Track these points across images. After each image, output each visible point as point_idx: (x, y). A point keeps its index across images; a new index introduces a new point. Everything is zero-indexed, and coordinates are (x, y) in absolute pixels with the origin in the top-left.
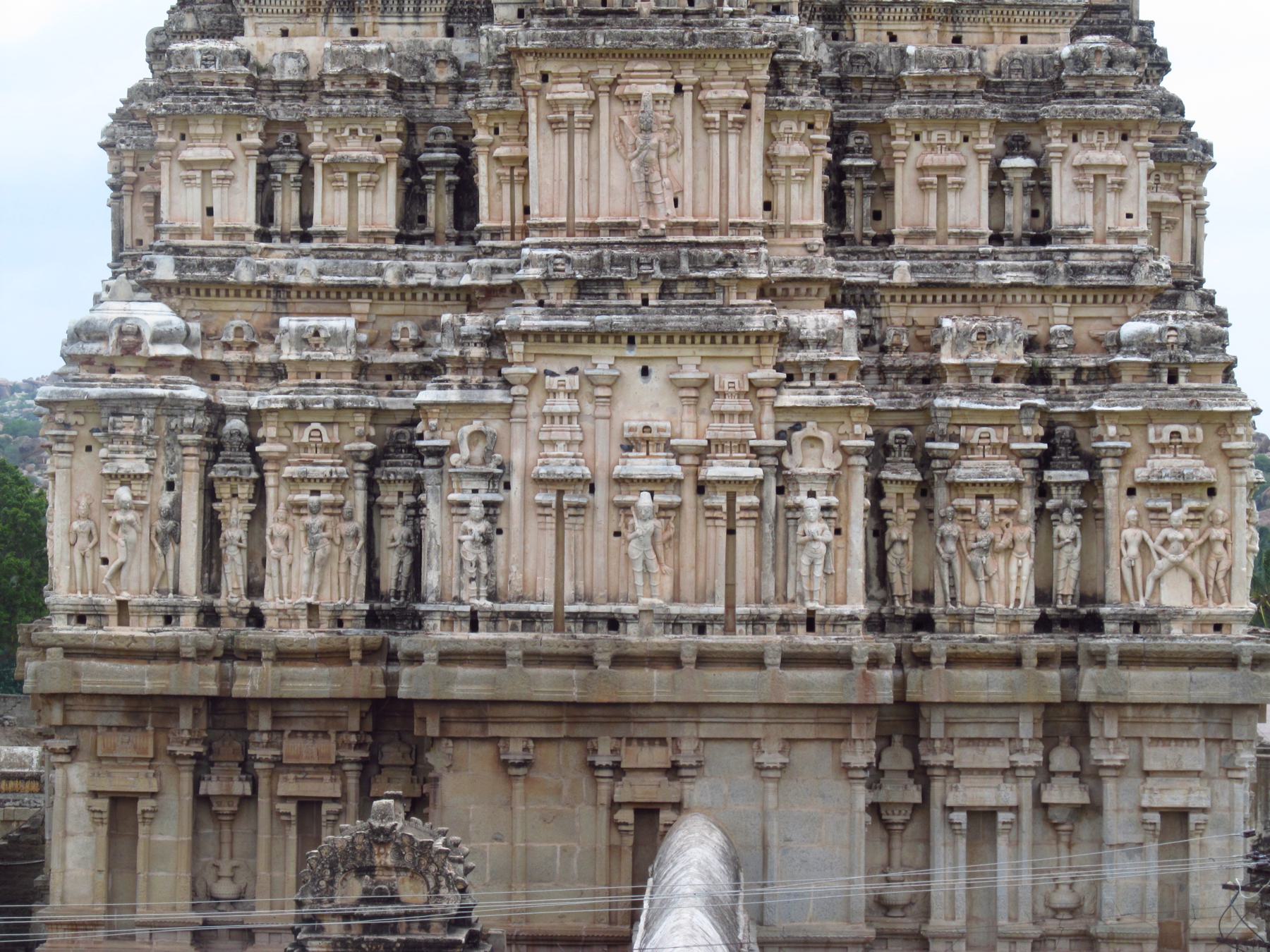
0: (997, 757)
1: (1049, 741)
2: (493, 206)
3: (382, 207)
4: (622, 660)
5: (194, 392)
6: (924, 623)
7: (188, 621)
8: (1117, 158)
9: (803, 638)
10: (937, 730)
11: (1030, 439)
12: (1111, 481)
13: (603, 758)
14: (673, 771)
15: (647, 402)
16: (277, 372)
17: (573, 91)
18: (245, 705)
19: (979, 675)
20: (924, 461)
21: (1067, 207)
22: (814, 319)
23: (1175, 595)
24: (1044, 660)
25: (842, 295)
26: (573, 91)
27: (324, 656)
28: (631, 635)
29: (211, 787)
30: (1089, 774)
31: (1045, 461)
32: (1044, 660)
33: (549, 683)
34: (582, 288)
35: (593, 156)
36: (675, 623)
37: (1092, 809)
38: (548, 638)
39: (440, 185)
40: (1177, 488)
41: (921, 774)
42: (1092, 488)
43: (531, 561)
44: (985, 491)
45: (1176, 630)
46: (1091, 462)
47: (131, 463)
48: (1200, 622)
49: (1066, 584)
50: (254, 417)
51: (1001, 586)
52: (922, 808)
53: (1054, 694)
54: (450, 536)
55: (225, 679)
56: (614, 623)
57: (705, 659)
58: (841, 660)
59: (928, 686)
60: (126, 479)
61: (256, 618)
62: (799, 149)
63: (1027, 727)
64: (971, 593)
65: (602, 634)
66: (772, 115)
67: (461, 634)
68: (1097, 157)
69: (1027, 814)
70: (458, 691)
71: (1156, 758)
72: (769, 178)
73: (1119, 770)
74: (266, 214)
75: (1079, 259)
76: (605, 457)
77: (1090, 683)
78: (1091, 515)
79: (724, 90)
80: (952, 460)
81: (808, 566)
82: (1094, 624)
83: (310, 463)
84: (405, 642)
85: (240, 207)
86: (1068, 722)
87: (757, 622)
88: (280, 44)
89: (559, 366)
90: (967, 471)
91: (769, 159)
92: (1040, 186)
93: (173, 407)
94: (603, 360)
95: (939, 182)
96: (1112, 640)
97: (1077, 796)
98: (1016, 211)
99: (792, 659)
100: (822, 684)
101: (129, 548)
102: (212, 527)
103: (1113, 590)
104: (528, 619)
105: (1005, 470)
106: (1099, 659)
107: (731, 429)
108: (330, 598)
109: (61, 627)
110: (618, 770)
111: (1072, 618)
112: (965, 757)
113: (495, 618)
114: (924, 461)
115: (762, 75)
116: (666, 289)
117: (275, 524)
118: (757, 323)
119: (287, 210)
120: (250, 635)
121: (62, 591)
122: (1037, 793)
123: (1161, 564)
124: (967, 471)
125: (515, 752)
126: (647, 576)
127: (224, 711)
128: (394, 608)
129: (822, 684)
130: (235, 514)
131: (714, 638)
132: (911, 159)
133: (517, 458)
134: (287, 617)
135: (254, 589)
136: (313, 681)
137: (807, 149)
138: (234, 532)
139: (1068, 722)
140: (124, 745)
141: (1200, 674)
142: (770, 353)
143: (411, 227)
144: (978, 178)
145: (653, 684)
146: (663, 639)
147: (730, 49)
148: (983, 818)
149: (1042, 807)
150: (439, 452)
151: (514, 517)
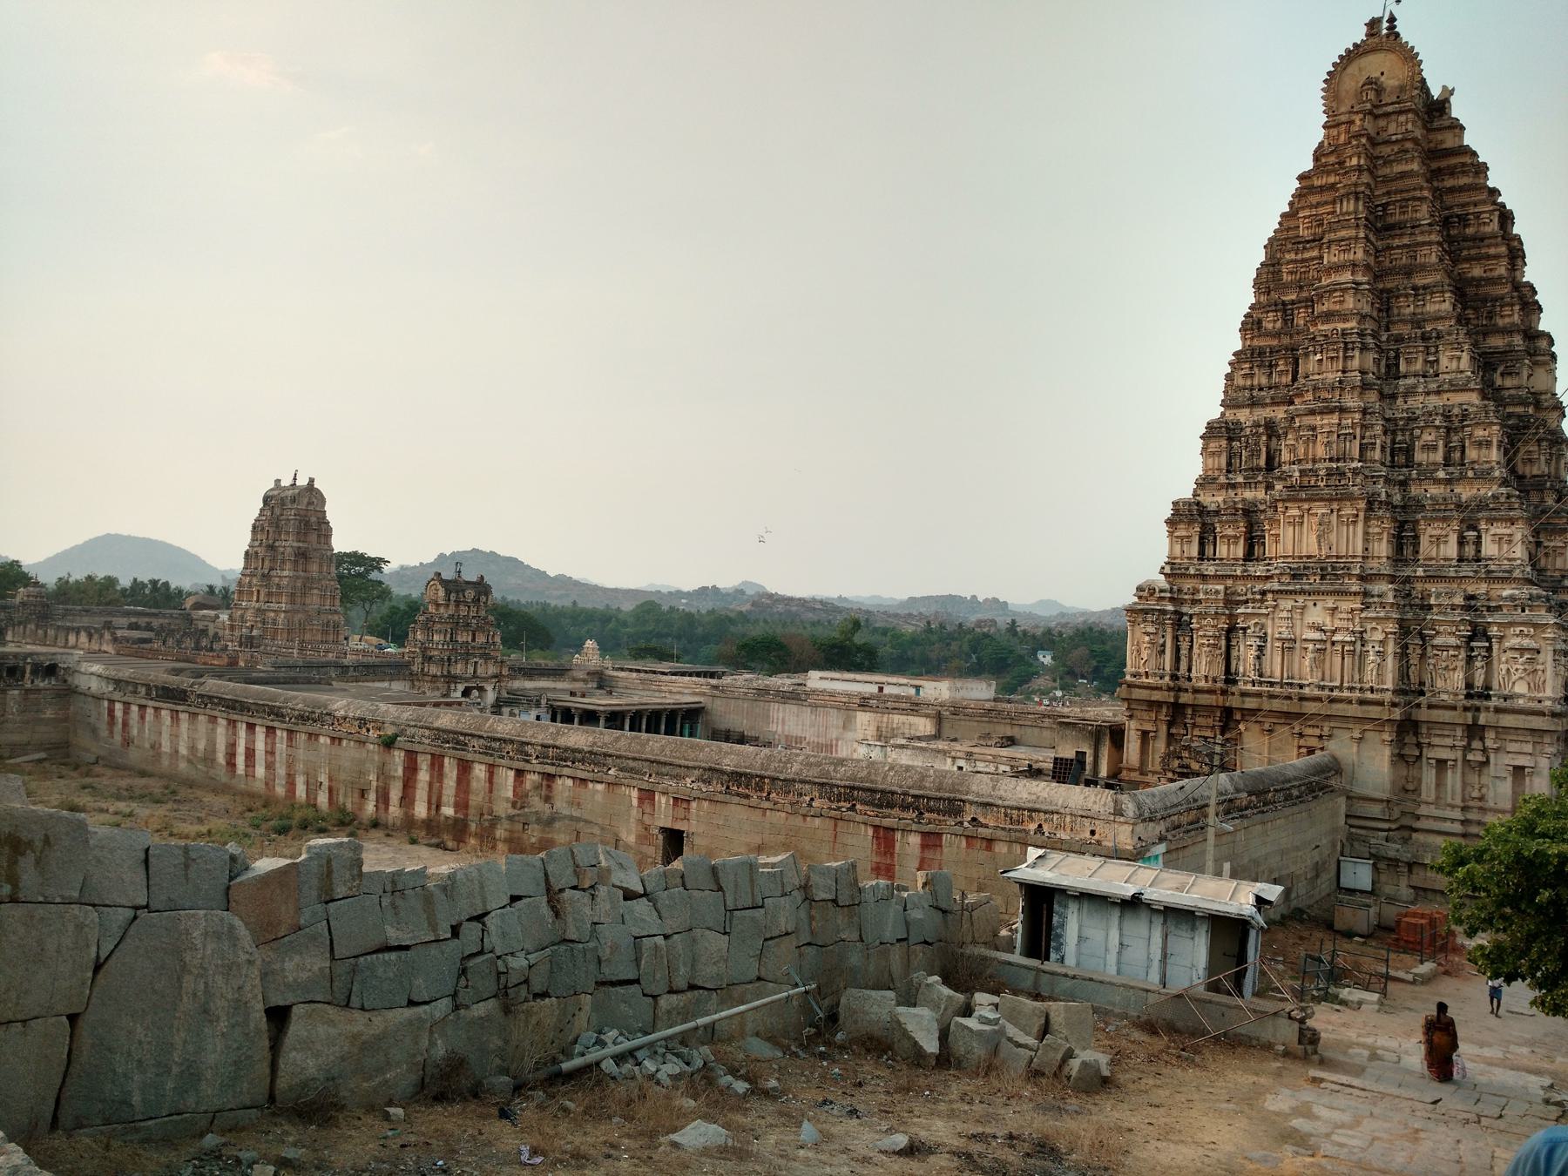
0: (1449, 741)
1: (1470, 738)
3: (1239, 551)
4: (1302, 699)
5: (1170, 608)
6: (1422, 693)
7: (1167, 678)
8: (1508, 531)
9: (1369, 695)
10: (1424, 730)
11: (1465, 631)
12: (1495, 647)
13: (1297, 730)
14: (1321, 737)
15: (1317, 614)
17: (1295, 512)
18: (1184, 706)
19: (1440, 712)
20: (1422, 637)
21: (1489, 548)
23: (1521, 688)
24: (1466, 709)
25: (1392, 579)
26: (1295, 512)
27: (1210, 692)
28: (1306, 691)
29: (1173, 731)
31: (1471, 639)
32: (1466, 709)
33: (1276, 705)
34: (1294, 577)
35: (1301, 533)
36: (1323, 688)
37: (1487, 762)
38: (1277, 689)
40: (1522, 650)
41: (1419, 745)
42: (1489, 649)
43: (1274, 665)
44: (1446, 648)
45: (1521, 701)
46: (1489, 639)
47: (1151, 629)
48: (1531, 699)
49: (1479, 681)
50: (1191, 616)
51: (1450, 682)
52: (1419, 757)
53: (1470, 722)
54: (1246, 654)
55: (1177, 698)
56: (1301, 686)
57: (1333, 701)
58: (1380, 703)
59: (1423, 715)
60: (1148, 634)
61: (1190, 679)
62: (1377, 530)
63: (1459, 732)
64: (1440, 684)
65: (1297, 690)
66: (1367, 519)
67: (1249, 687)
68: (1499, 531)
69: (1459, 763)
70: (1247, 706)
71: (1513, 747)
72: (1366, 540)
73: (1497, 750)
74: (1202, 552)
75: (1493, 568)
77: (1483, 719)
79: (1348, 511)
80: (1433, 637)
81: (1370, 668)
82: (1488, 697)
83: (1206, 632)
84: (1234, 689)
86: (1474, 731)
87: (1351, 689)
88: (1210, 499)
89: (1287, 604)
90: (1438, 641)
91: (1366, 533)
92: (1478, 542)
93: (1163, 612)
94: (1301, 599)
95: (1438, 540)
96: (1494, 702)
97: (1480, 757)
98: (1470, 551)
99: (1362, 702)
100: (1374, 712)
102: (1177, 650)
103: (1495, 685)
104: (1272, 684)
105: (1452, 641)
106: (1487, 709)
107: (1344, 624)
108: (1211, 675)
109: (1128, 678)
110: (1301, 735)
111: (1477, 694)
112: (1436, 741)
113: (1261, 683)
114: (1422, 637)
115: (1362, 505)
116: (1323, 577)
117: (1196, 650)
118: (1354, 588)
119: (1209, 551)
120: (1187, 685)
121: (1129, 669)
122: (1464, 756)
123: (1514, 678)
124: (1438, 641)
125: (1267, 726)
128: (1230, 678)
130: (1184, 646)
131: (1336, 693)
132: (1428, 532)
133: (1269, 631)
134: (1198, 679)
135: (1190, 670)
136: (1204, 699)
137: (1383, 528)
138: (1184, 652)
139: (1474, 731)
140: (1145, 716)
141: (1530, 718)
142: (1359, 599)
144: (1453, 538)
145: (1311, 708)
146: (1317, 692)
147: (1350, 498)
148: (1441, 764)
149: (1466, 761)
150: (1244, 629)
151: (1268, 651)
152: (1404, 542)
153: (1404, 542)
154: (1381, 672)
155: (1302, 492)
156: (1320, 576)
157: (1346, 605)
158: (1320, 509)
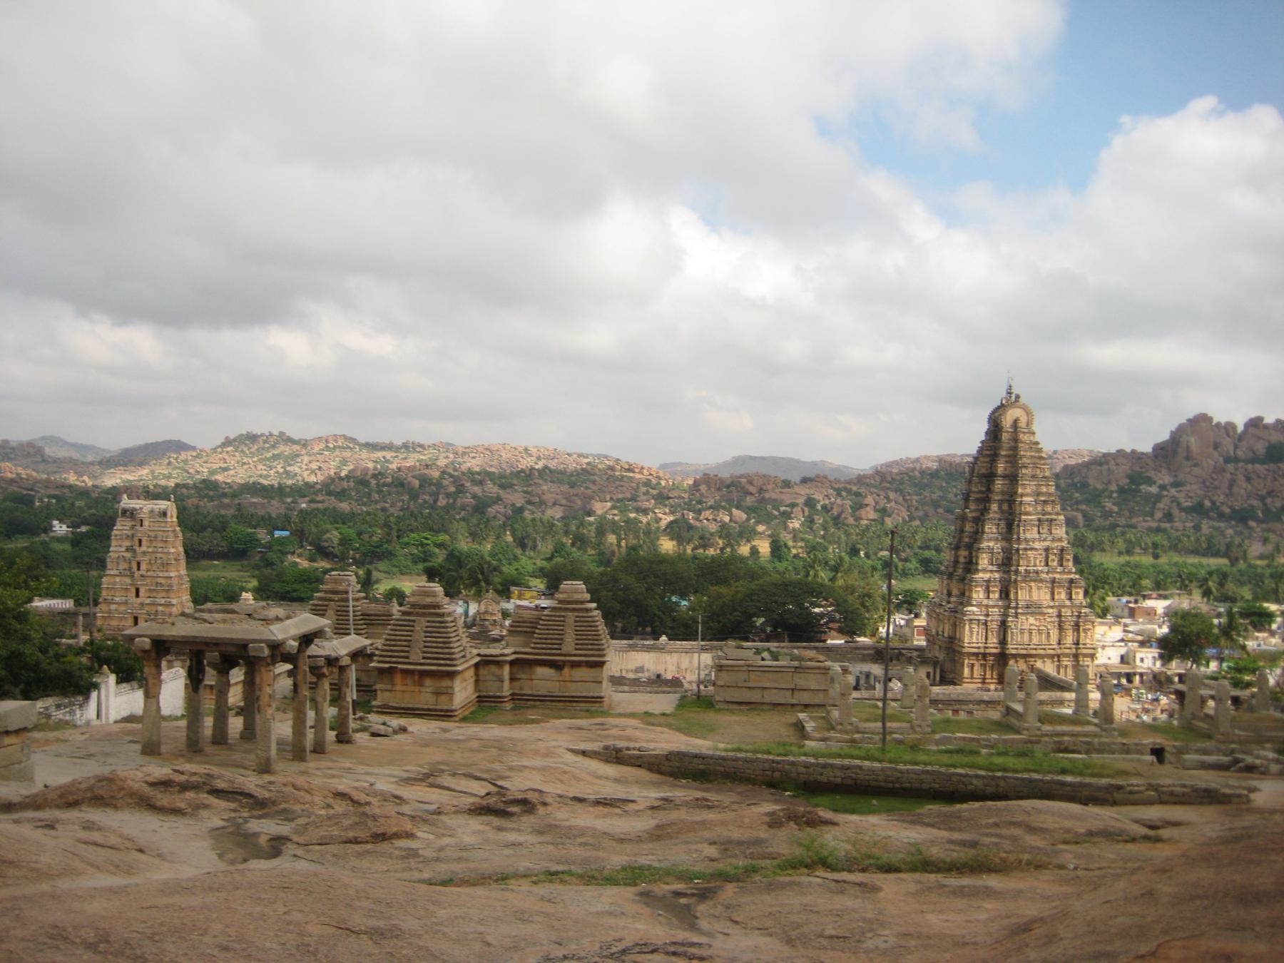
2: (1012, 596)
3: (997, 595)
15: (1032, 620)
22: (1050, 611)
33: (1024, 652)
85: (981, 595)
86: (1076, 656)
92: (1071, 594)
95: (1059, 593)
127: (985, 655)
128: (1003, 642)
129: (1052, 652)
139: (1076, 656)
143: (1001, 598)
145: (1033, 652)
147: (1041, 581)
152: (1053, 593)
153: (1053, 593)
156: (1033, 608)
158: (1032, 584)
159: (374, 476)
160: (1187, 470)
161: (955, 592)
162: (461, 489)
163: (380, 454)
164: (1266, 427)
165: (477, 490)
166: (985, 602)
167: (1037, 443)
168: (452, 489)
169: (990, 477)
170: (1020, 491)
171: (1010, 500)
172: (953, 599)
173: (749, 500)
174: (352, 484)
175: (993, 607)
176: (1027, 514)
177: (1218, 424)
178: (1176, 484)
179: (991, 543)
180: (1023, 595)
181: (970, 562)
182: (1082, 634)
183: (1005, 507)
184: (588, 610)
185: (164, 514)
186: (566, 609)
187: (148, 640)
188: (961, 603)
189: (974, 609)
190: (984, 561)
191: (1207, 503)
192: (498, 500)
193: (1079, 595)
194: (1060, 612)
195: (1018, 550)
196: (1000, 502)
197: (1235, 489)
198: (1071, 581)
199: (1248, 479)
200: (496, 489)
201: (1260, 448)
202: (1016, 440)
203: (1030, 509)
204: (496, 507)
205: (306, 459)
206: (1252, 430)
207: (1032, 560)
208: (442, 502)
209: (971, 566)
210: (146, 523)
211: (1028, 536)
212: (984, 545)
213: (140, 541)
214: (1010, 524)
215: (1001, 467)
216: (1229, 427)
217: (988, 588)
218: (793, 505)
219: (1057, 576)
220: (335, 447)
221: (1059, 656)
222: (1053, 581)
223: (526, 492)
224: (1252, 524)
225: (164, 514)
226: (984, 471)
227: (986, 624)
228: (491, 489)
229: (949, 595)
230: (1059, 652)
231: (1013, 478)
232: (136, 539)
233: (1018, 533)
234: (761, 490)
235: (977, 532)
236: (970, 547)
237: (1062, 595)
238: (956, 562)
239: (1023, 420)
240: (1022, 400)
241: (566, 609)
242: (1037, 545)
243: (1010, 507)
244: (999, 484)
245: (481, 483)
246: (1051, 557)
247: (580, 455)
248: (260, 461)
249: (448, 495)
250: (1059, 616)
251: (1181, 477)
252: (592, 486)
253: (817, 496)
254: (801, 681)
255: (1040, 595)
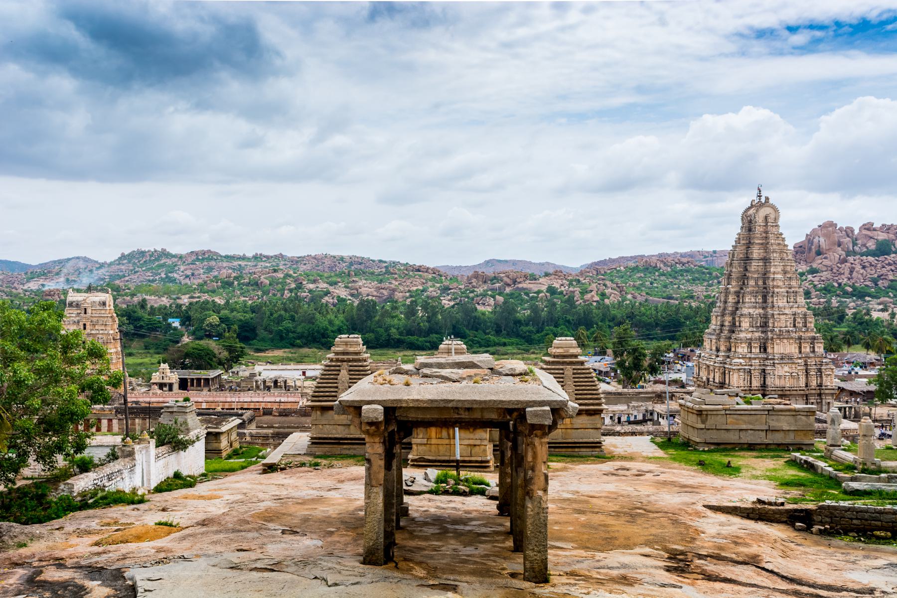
2: (769, 350)
3: (758, 350)
15: (786, 369)
16: (751, 365)
22: (800, 361)
30: (821, 399)
39: (764, 349)
43: (778, 382)
51: (814, 383)
76: (784, 373)
78: (821, 377)
83: (756, 373)
85: (746, 350)
86: (820, 395)
92: (814, 348)
101: (741, 381)
126: (788, 383)
129: (802, 392)
132: (803, 345)
139: (820, 395)
145: (788, 393)
147: (792, 338)
152: (800, 348)
153: (800, 348)
154: (802, 382)
155: (780, 336)
157: (793, 366)
158: (785, 341)
159: (236, 278)
160: (820, 261)
161: (722, 348)
162: (300, 286)
163: (236, 263)
164: (875, 230)
165: (311, 286)
166: (749, 355)
167: (781, 234)
168: (293, 286)
169: (747, 259)
170: (772, 270)
171: (765, 276)
172: (720, 354)
173: (508, 290)
174: (219, 284)
175: (755, 359)
176: (778, 287)
177: (841, 229)
178: (813, 271)
179: (750, 308)
180: (779, 348)
181: (734, 324)
182: (824, 378)
183: (760, 283)
184: (582, 363)
185: (104, 304)
186: (563, 363)
187: (380, 408)
188: (728, 357)
189: (741, 361)
190: (745, 324)
191: (836, 284)
192: (327, 293)
193: (820, 348)
194: (806, 361)
195: (773, 315)
196: (756, 280)
197: (854, 274)
198: (814, 338)
199: (864, 267)
200: (325, 285)
201: (871, 245)
202: (766, 232)
203: (780, 284)
204: (326, 298)
205: (182, 268)
206: (865, 232)
207: (782, 322)
208: (287, 294)
209: (734, 328)
210: (89, 311)
211: (781, 305)
212: (745, 311)
213: (85, 325)
214: (765, 294)
215: (756, 253)
216: (849, 232)
217: (750, 344)
218: (539, 292)
219: (801, 334)
220: (203, 259)
221: (807, 395)
222: (800, 338)
223: (346, 287)
224: (867, 298)
225: (104, 304)
226: (741, 256)
227: (750, 371)
228: (323, 285)
229: (718, 350)
230: (807, 392)
231: (766, 260)
232: (81, 324)
233: (773, 302)
234: (515, 282)
235: (738, 302)
236: (733, 314)
237: (807, 349)
238: (722, 325)
239: (772, 216)
240: (771, 201)
241: (563, 363)
242: (787, 311)
243: (764, 283)
244: (755, 266)
245: (315, 281)
246: (798, 320)
247: (380, 261)
248: (148, 270)
249: (291, 291)
250: (806, 365)
251: (815, 265)
252: (394, 282)
253: (556, 285)
254: (774, 424)
255: (791, 348)
